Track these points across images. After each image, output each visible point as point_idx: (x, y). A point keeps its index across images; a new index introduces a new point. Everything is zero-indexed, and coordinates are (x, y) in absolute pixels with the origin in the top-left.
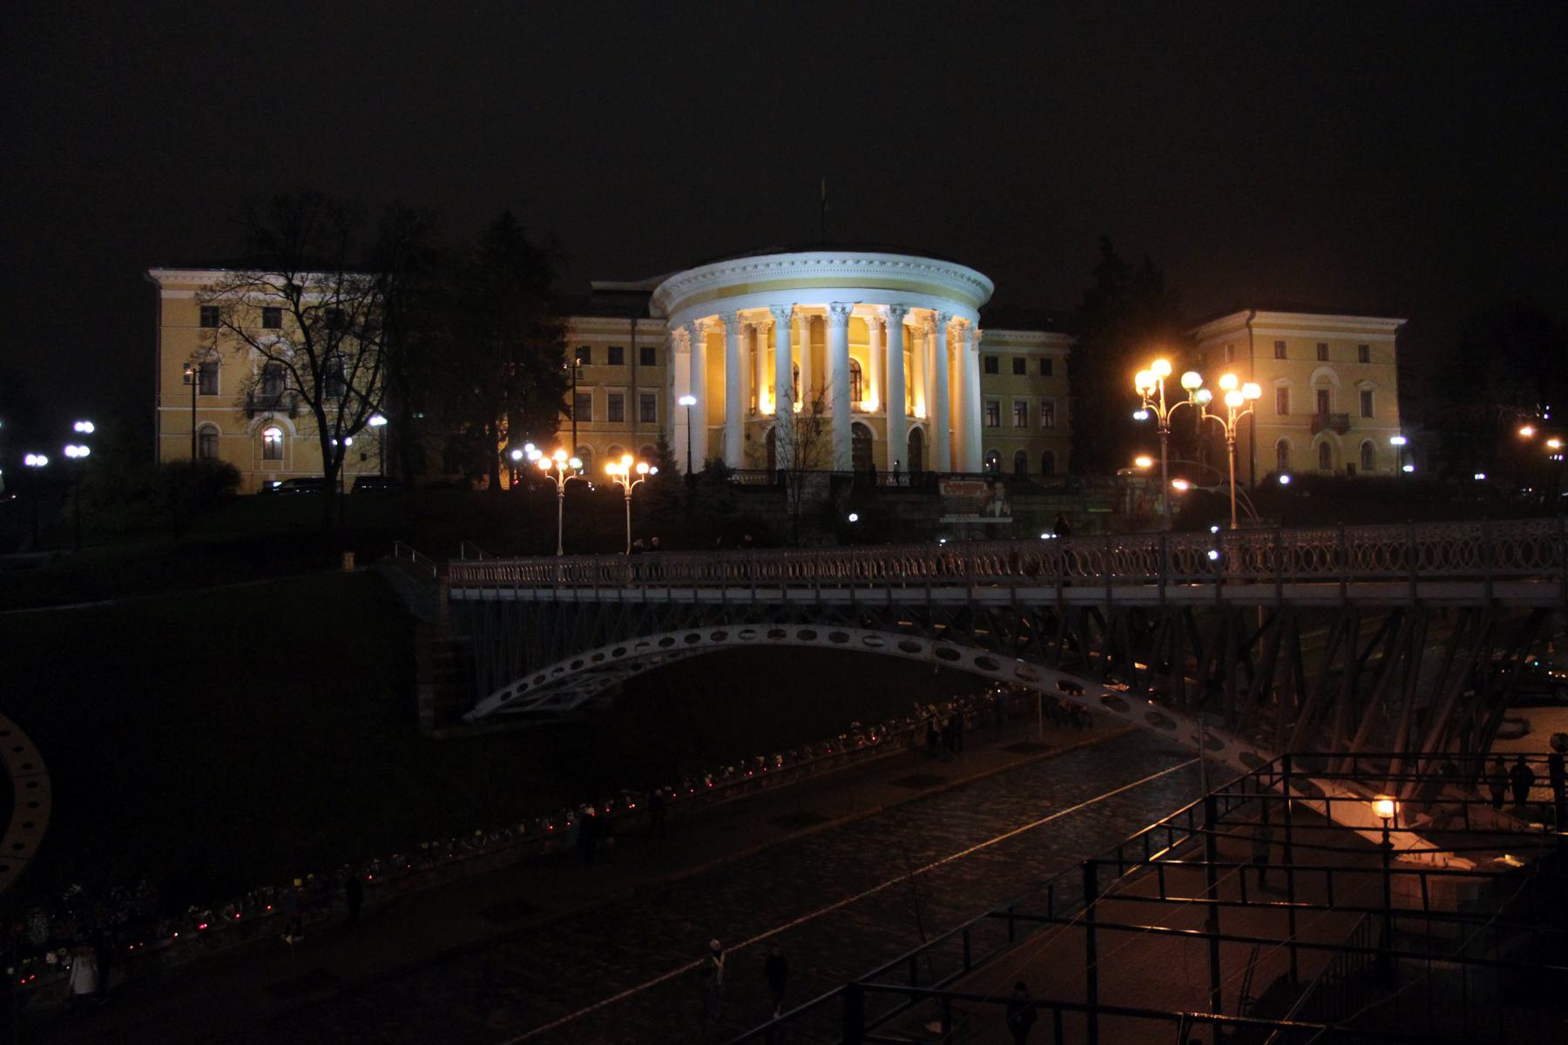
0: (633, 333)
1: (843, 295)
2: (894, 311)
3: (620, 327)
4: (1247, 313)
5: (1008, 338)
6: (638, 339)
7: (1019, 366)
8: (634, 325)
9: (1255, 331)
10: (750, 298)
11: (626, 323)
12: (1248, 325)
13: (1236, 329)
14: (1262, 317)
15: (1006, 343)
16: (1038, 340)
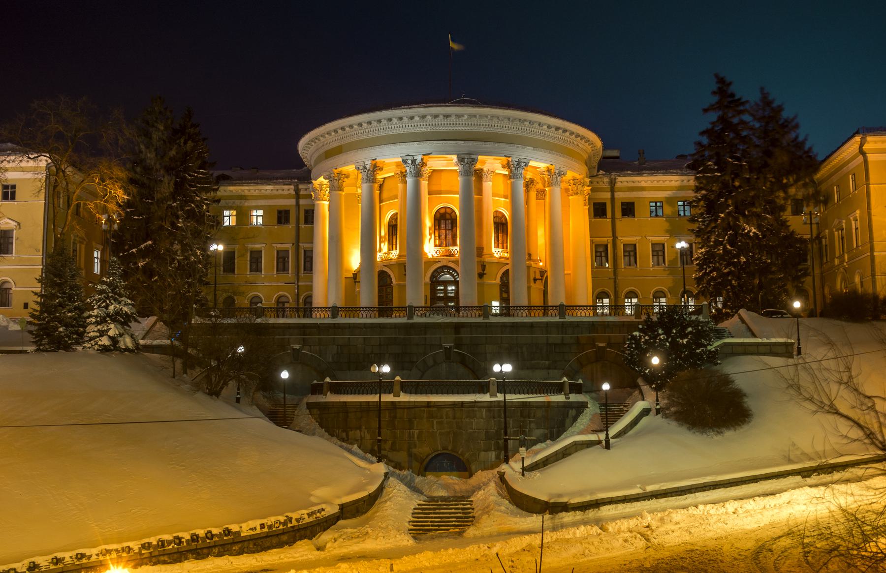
0: (298, 196)
1: (415, 150)
2: (461, 160)
3: (286, 192)
4: (858, 138)
5: (643, 184)
6: (302, 202)
7: (657, 209)
8: (297, 191)
9: (870, 157)
10: (343, 157)
11: (289, 189)
12: (862, 152)
13: (854, 158)
14: (873, 143)
15: (642, 189)
16: (674, 184)
